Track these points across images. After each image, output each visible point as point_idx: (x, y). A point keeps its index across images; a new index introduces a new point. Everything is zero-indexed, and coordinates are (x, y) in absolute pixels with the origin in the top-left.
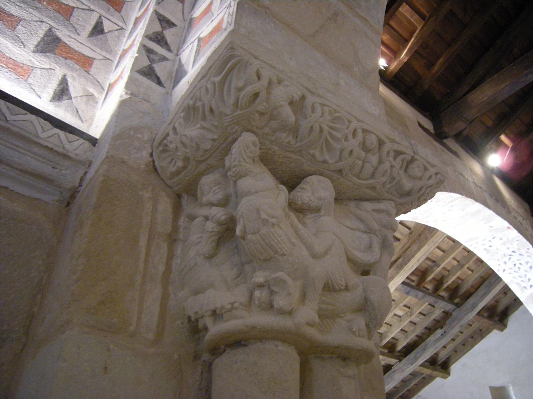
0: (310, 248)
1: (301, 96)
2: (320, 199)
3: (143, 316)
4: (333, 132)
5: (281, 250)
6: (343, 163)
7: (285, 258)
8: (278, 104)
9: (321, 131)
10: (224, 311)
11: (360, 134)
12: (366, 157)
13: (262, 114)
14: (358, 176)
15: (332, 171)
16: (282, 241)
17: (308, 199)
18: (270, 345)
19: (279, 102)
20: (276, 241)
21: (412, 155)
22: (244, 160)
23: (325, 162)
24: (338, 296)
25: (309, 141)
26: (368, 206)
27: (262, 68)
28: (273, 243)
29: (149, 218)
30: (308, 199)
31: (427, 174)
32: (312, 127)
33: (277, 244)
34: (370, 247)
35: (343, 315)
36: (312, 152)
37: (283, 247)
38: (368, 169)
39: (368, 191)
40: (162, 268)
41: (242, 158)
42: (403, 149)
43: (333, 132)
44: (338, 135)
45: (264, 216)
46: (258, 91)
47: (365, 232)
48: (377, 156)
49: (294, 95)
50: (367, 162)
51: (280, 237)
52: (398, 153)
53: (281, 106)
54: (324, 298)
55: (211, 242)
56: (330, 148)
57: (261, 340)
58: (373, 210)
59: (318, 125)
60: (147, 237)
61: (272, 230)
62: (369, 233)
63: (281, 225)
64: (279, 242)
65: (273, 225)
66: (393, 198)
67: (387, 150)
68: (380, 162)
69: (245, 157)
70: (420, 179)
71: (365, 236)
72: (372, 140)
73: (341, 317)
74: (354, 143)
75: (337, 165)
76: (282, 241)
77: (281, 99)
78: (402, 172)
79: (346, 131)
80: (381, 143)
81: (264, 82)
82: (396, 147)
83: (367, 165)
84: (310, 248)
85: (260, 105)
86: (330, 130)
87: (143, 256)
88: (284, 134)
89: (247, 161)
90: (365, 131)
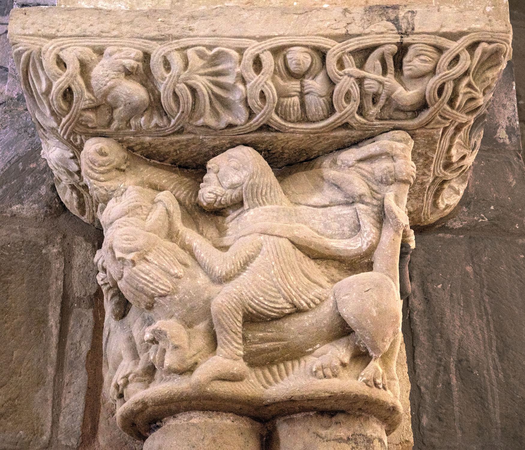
0: (209, 272)
1: (141, 54)
2: (233, 187)
3: (61, 418)
4: (221, 79)
5: (156, 291)
6: (258, 116)
7: (168, 298)
8: (104, 88)
9: (193, 90)
10: (120, 388)
11: (268, 59)
12: (302, 86)
13: (95, 108)
14: (305, 119)
15: (256, 131)
16: (152, 278)
17: (212, 196)
18: (181, 420)
19: (105, 85)
20: (144, 281)
21: (398, 40)
22: (96, 179)
23: (230, 126)
24: (286, 324)
25: (183, 112)
26: (350, 155)
27: (61, 50)
28: (141, 285)
29: (60, 283)
30: (212, 196)
31: (446, 58)
32: (174, 93)
33: (148, 286)
34: (357, 228)
35: (310, 350)
36: (200, 122)
37: (157, 287)
38: (316, 103)
39: (341, 133)
40: (85, 347)
41: (92, 178)
42: (368, 41)
43: (221, 79)
44: (229, 80)
45: (118, 254)
46: (66, 86)
47: (347, 204)
48: (321, 77)
49: (126, 62)
50: (308, 93)
51: (147, 274)
52: (363, 54)
53: (112, 88)
54: (261, 334)
55: (112, 298)
56: (226, 105)
57: (173, 414)
58: (361, 160)
59: (182, 86)
60: (58, 310)
61: (134, 268)
62: (353, 202)
63: (148, 258)
64: (149, 281)
65: (133, 262)
66: (397, 123)
67: (335, 59)
68: (331, 83)
69: (96, 175)
70: (433, 72)
71: (347, 211)
72: (299, 58)
73: (310, 353)
74: (265, 81)
75: (252, 122)
76: (152, 278)
77: (107, 79)
78: (390, 79)
79: (238, 70)
80: (321, 54)
81: (73, 67)
82: (354, 44)
83: (308, 98)
84: (209, 272)
85: (83, 98)
86: (215, 79)
87: (54, 340)
88: (143, 119)
89: (101, 179)
90: (276, 51)
